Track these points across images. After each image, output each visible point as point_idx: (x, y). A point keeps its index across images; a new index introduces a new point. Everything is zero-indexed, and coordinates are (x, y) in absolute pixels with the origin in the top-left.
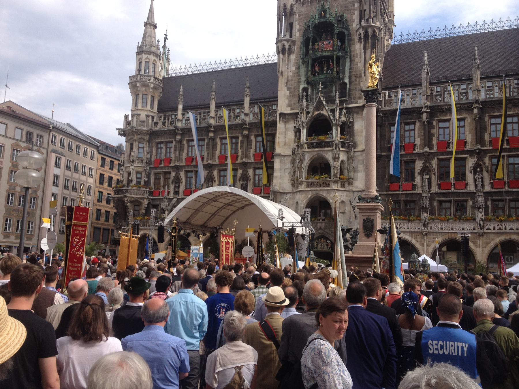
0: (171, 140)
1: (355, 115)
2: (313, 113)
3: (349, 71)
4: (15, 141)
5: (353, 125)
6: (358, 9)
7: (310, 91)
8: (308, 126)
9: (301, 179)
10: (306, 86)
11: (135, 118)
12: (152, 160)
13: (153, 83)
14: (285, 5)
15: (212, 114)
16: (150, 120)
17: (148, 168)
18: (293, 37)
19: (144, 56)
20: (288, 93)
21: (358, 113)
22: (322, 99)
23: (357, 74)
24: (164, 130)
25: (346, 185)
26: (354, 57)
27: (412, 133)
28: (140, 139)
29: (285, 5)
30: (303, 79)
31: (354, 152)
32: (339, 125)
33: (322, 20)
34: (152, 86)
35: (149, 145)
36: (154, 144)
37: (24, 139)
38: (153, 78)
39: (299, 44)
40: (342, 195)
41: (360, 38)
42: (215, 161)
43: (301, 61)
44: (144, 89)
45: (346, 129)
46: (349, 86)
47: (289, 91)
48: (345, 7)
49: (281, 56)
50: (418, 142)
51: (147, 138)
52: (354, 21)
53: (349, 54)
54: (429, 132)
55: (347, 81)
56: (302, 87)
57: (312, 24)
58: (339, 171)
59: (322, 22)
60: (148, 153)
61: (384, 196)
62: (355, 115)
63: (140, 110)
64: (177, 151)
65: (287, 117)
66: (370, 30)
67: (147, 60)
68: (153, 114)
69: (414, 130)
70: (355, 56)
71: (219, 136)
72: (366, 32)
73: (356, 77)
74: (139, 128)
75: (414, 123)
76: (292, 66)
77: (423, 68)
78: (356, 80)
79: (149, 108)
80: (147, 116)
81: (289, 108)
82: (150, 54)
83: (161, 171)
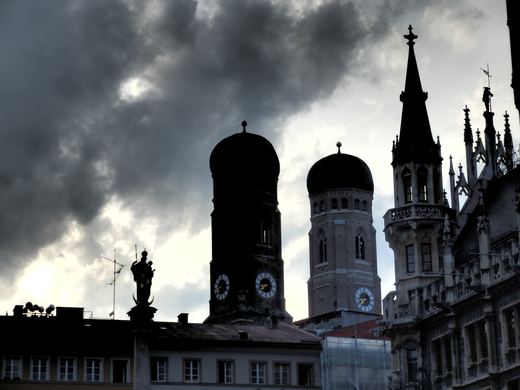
12: (432, 382)
13: (415, 220)
15: (485, 263)
24: (435, 315)
28: (407, 341)
34: (414, 226)
35: (424, 350)
37: (271, 382)
38: (413, 210)
44: (405, 235)
51: (417, 337)
63: (403, 280)
67: (408, 174)
71: (502, 309)
74: (399, 321)
80: (410, 292)
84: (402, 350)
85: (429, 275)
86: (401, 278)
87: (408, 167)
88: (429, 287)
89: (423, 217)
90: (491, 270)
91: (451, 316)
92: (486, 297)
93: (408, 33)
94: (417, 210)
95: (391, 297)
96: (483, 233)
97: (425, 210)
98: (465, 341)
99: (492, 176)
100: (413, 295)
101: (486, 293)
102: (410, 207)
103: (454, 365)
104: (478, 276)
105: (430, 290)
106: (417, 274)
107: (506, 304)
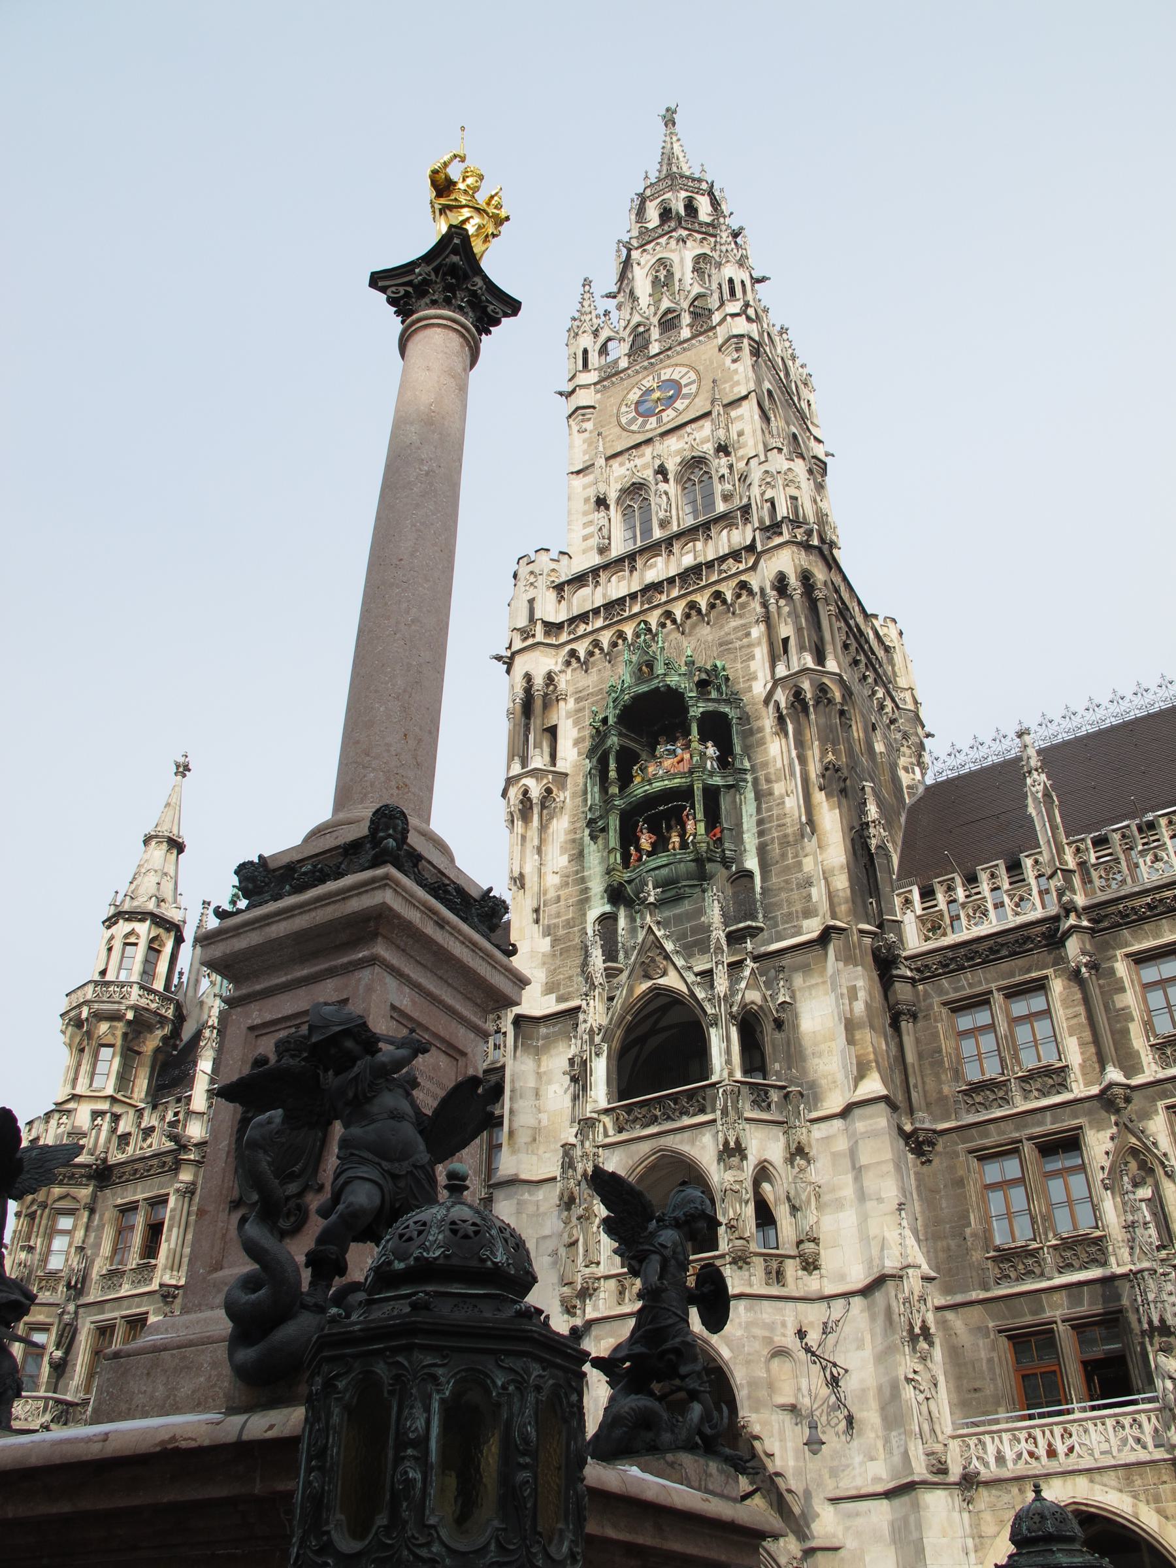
0: (163, 1191)
1: (798, 980)
2: (631, 990)
3: (755, 830)
5: (796, 1016)
6: (764, 641)
7: (622, 922)
8: (616, 1044)
9: (593, 1269)
10: (607, 908)
11: (53, 1122)
12: (94, 1274)
13: (135, 1008)
14: (528, 677)
16: (105, 1124)
17: (71, 1308)
18: (559, 763)
19: (123, 927)
20: (545, 944)
21: (805, 968)
22: (658, 934)
23: (786, 836)
25: (791, 1269)
26: (768, 781)
27: (1042, 1028)
29: (528, 677)
30: (597, 886)
31: (813, 1121)
33: (644, 688)
36: (107, 1214)
38: (135, 990)
39: (581, 780)
41: (781, 719)
43: (587, 832)
45: (763, 1036)
46: (764, 880)
47: (548, 939)
48: (721, 645)
49: (519, 824)
50: (1074, 1053)
52: (755, 678)
53: (749, 777)
54: (1107, 1008)
55: (752, 863)
56: (593, 914)
57: (615, 708)
58: (750, 1211)
59: (645, 694)
60: (81, 1249)
61: (977, 1312)
62: (798, 980)
64: (175, 1230)
65: (543, 1030)
66: (806, 685)
67: (132, 940)
68: (118, 1109)
69: (1047, 1013)
70: (773, 777)
72: (798, 694)
73: (785, 842)
75: (1040, 986)
76: (557, 850)
77: (1029, 781)
78: (784, 856)
80: (96, 1114)
81: (553, 996)
82: (142, 920)
83: (116, 1314)
86: (78, 1091)
87: (137, 930)
93: (181, 760)
94: (141, 993)
95: (57, 1116)
97: (152, 997)
106: (110, 1091)
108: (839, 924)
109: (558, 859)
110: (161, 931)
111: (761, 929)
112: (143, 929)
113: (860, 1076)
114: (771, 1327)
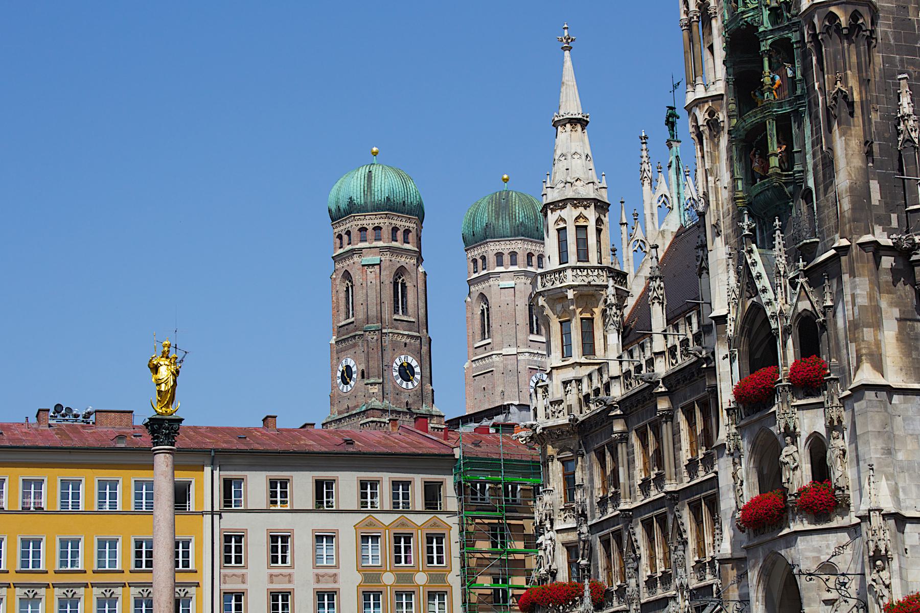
2: (743, 306)
4: (361, 517)
8: (744, 348)
15: (659, 344)
17: (585, 529)
19: (552, 217)
22: (749, 261)
32: (787, 331)
33: (733, 26)
34: (570, 294)
37: (388, 506)
40: (824, 543)
42: (681, 481)
55: (811, 183)
63: (557, 368)
67: (562, 225)
74: (551, 423)
79: (577, 356)
82: (562, 208)
84: (555, 460)
85: (592, 361)
88: (590, 376)
89: (583, 283)
90: (667, 354)
91: (616, 415)
92: (660, 390)
94: (574, 273)
96: (656, 304)
97: (585, 273)
98: (635, 447)
99: (678, 226)
100: (569, 388)
101: (661, 384)
102: (565, 269)
103: (621, 480)
104: (650, 363)
105: (591, 380)
107: (685, 400)
108: (845, 242)
109: (726, 178)
110: (581, 209)
111: (817, 242)
112: (570, 213)
113: (857, 368)
114: (819, 550)
